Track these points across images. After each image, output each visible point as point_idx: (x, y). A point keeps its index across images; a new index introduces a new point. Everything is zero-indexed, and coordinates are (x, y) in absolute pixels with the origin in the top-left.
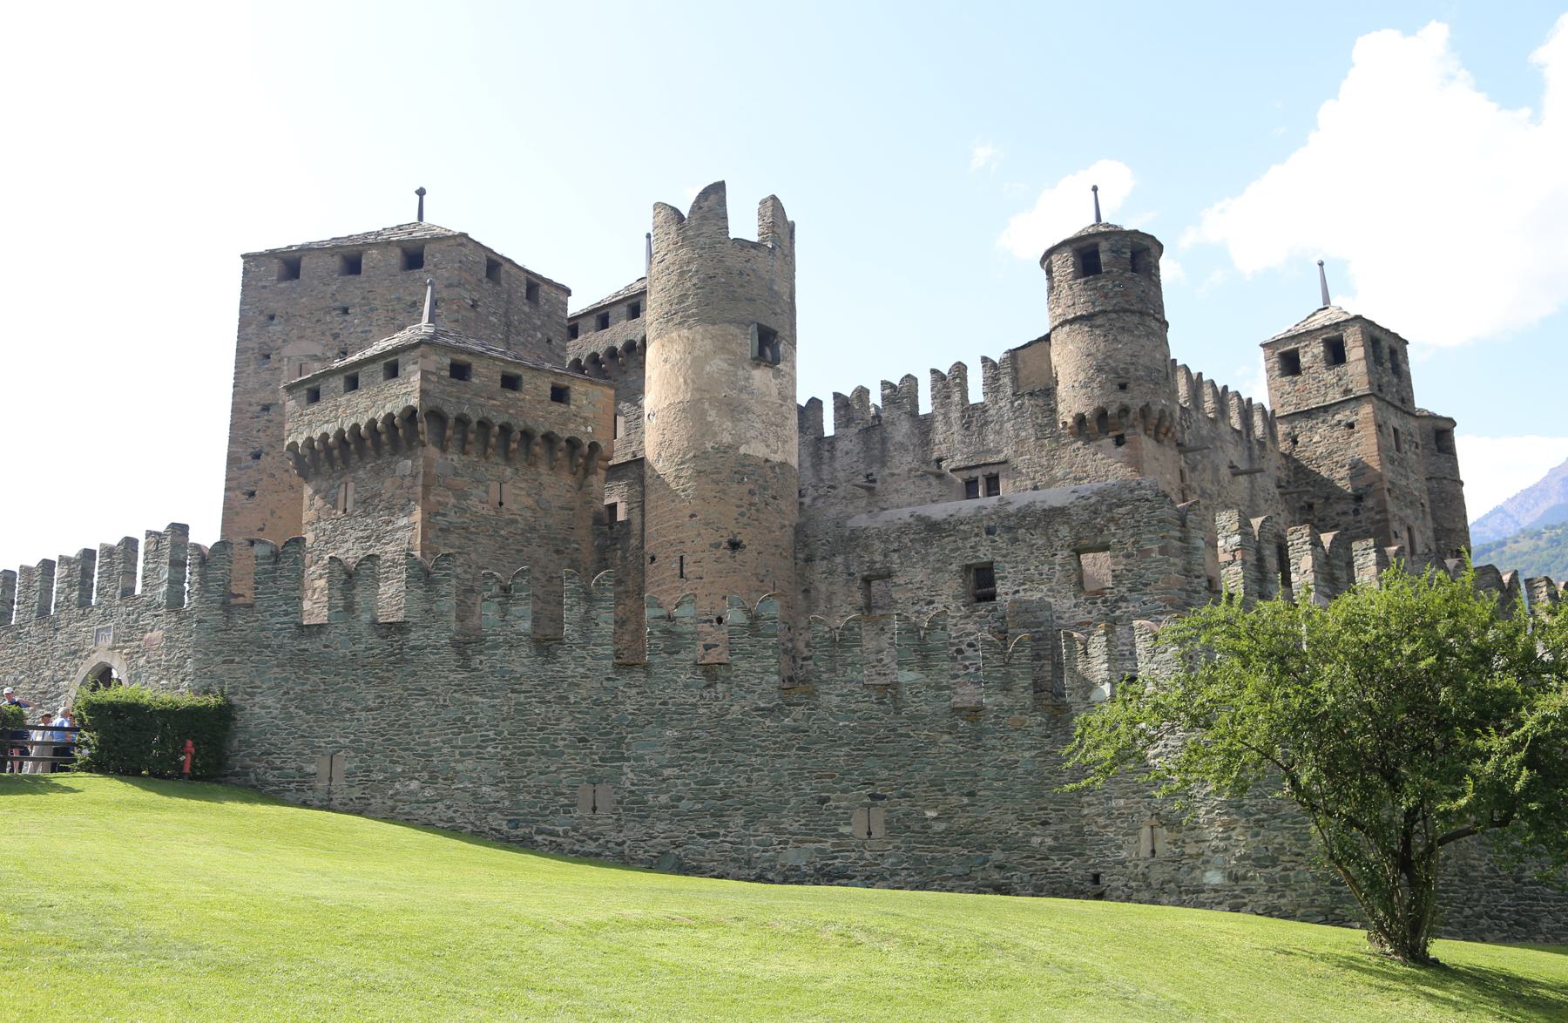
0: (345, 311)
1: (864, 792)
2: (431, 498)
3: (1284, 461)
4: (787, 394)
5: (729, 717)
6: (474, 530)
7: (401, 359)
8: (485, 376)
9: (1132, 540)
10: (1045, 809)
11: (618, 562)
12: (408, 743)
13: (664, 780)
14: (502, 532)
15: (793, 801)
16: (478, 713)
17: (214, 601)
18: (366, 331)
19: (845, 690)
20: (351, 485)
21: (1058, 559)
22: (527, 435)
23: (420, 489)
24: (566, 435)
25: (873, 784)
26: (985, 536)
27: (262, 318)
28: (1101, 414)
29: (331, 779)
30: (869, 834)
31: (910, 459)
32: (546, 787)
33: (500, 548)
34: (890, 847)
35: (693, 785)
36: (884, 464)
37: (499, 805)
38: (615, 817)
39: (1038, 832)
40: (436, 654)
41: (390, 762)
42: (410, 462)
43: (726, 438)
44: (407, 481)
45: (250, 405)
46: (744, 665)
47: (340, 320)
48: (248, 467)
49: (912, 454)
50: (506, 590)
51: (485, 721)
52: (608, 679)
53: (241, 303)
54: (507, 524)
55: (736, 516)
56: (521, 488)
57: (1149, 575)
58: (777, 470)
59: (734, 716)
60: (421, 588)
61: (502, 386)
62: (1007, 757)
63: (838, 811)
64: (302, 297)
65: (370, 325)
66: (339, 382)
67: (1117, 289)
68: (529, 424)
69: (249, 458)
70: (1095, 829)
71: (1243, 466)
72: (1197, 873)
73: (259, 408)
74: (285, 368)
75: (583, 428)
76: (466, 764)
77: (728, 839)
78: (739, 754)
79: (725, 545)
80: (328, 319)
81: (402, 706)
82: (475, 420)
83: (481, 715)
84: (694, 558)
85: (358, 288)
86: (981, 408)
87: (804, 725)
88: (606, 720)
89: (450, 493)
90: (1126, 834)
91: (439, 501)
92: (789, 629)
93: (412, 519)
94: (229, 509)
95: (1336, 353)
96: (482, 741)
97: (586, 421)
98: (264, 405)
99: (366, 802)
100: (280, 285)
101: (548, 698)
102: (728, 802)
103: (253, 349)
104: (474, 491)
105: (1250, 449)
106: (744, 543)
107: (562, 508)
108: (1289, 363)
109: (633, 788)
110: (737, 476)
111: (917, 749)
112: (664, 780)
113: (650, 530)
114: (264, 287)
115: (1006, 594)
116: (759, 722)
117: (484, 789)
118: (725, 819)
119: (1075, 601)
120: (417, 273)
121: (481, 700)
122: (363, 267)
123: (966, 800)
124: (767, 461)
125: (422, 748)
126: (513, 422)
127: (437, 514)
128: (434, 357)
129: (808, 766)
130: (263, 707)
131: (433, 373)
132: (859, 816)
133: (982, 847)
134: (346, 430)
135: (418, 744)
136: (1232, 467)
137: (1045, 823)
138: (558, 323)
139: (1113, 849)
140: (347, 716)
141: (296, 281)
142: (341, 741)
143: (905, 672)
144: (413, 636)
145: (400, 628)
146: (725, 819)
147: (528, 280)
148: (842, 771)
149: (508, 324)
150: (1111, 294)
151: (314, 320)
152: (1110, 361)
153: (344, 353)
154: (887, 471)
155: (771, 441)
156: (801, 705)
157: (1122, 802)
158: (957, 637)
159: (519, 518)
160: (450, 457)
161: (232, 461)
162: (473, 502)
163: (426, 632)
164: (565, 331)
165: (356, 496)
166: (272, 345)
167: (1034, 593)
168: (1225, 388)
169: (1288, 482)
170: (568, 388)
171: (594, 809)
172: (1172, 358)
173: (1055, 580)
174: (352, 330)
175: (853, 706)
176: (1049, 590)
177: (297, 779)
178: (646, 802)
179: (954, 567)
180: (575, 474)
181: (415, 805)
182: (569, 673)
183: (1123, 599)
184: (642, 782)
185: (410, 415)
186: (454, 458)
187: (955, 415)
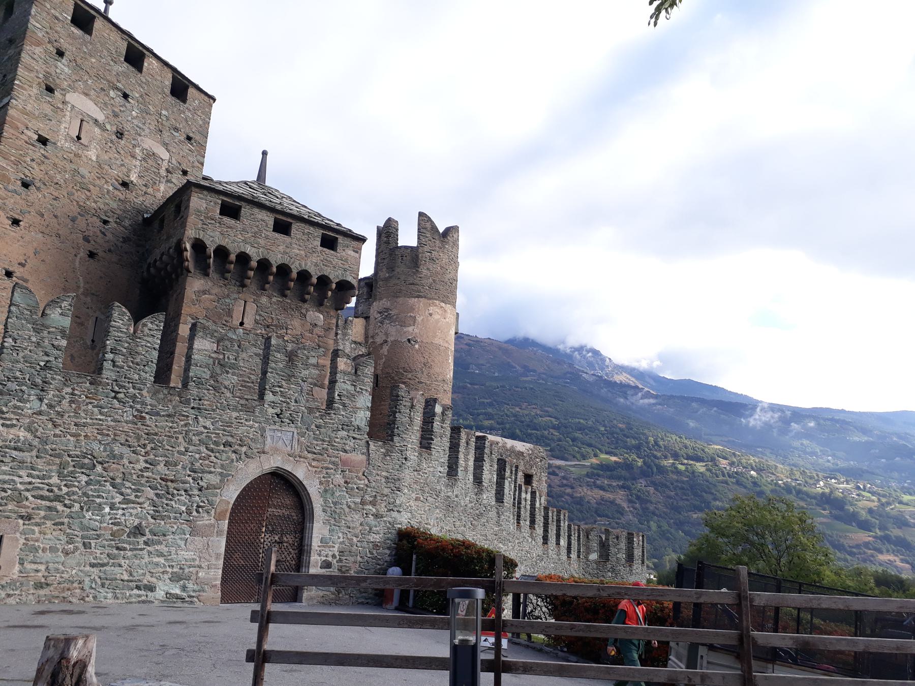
7: (341, 239)
20: (251, 308)
42: (322, 316)
44: (317, 330)
47: (122, 100)
48: (15, 192)
64: (91, 56)
65: (144, 124)
66: (269, 219)
69: (19, 183)
74: (68, 113)
80: (112, 93)
85: (140, 85)
98: (39, 135)
114: (57, 18)
120: (182, 106)
122: (144, 69)
134: (273, 262)
141: (87, 37)
153: (122, 134)
165: (258, 318)
166: (58, 81)
174: (130, 118)
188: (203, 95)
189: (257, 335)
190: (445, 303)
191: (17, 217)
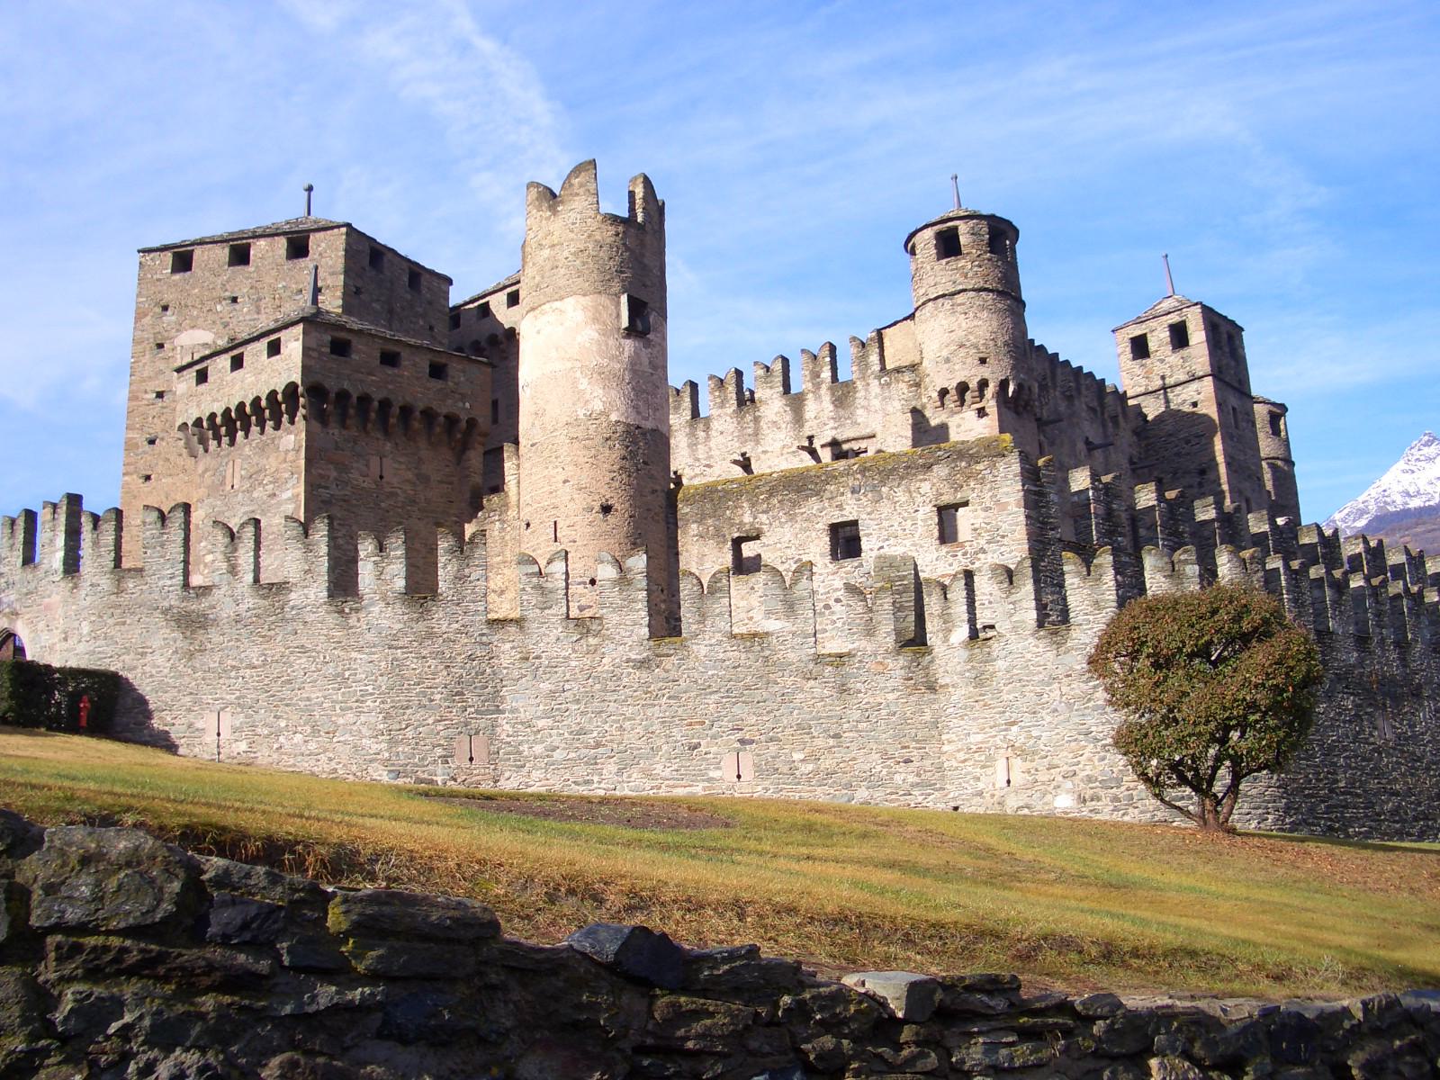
0: (234, 300)
1: (733, 737)
2: (313, 471)
3: (1135, 438)
4: (659, 365)
5: (599, 669)
6: (354, 502)
8: (363, 353)
9: (990, 494)
10: (907, 747)
11: (496, 533)
12: (291, 699)
13: (539, 731)
14: (383, 505)
15: (665, 747)
16: (356, 669)
17: (106, 566)
18: (254, 320)
19: (713, 641)
21: (920, 515)
22: (406, 411)
23: (303, 462)
24: (444, 411)
25: (742, 730)
26: (849, 495)
27: (159, 310)
28: (963, 388)
29: (219, 734)
30: (739, 777)
31: (783, 437)
32: (424, 739)
33: (381, 520)
34: (760, 788)
35: (566, 735)
36: (758, 442)
37: (379, 757)
38: (493, 767)
39: (900, 770)
40: (314, 613)
41: (275, 717)
43: (598, 406)
44: (291, 456)
45: (146, 392)
46: (615, 618)
48: (145, 453)
49: (784, 431)
50: (381, 548)
51: (364, 676)
52: (483, 635)
53: (137, 296)
54: (388, 497)
55: (607, 480)
56: (400, 463)
57: (1004, 526)
58: (648, 436)
59: (606, 668)
60: (300, 549)
61: (381, 363)
62: (871, 700)
63: (708, 756)
64: (194, 288)
66: (224, 361)
67: (975, 269)
68: (408, 399)
69: (146, 443)
70: (955, 764)
71: (1097, 440)
72: (1049, 797)
73: (154, 395)
74: (178, 356)
75: (461, 404)
76: (347, 717)
77: (602, 785)
78: (612, 704)
79: (597, 508)
80: (219, 308)
81: (284, 663)
82: (355, 397)
83: (360, 670)
84: (568, 523)
85: (247, 278)
86: (849, 386)
87: (673, 675)
88: (483, 673)
89: (331, 467)
90: (983, 767)
91: (320, 474)
92: (662, 591)
93: (296, 491)
94: (127, 493)
95: (1179, 336)
96: (362, 696)
97: (463, 397)
99: (252, 755)
100: (177, 277)
101: (424, 652)
102: (601, 750)
103: (148, 339)
104: (355, 465)
105: (1104, 426)
106: (617, 506)
107: (441, 482)
108: (1140, 348)
109: (509, 739)
110: (609, 442)
111: (783, 695)
112: (539, 731)
113: (525, 498)
114: (159, 280)
115: (871, 550)
116: (629, 674)
117: (364, 740)
118: (599, 766)
119: (936, 554)
120: (302, 262)
121: (359, 656)
122: (252, 258)
123: (831, 742)
124: (638, 427)
125: (304, 703)
126: (392, 397)
127: (320, 486)
128: (314, 334)
129: (679, 713)
130: (155, 666)
131: (314, 350)
132: (729, 762)
133: (849, 786)
135: (300, 700)
136: (1088, 442)
137: (908, 761)
138: (440, 311)
139: (971, 782)
140: (233, 674)
141: (189, 273)
142: (228, 697)
143: (772, 621)
144: (293, 596)
145: (280, 588)
146: (599, 766)
147: (410, 269)
148: (711, 718)
149: (391, 311)
150: (970, 275)
151: (205, 310)
152: (971, 338)
154: (760, 449)
155: (642, 409)
156: (671, 655)
157: (980, 738)
158: (825, 593)
159: (399, 491)
160: (331, 432)
161: (130, 446)
162: (354, 475)
163: (306, 591)
164: (447, 318)
165: (243, 472)
166: (166, 334)
167: (898, 548)
168: (1080, 368)
169: (1140, 459)
170: (445, 365)
171: (471, 759)
172: (1029, 337)
173: (917, 535)
174: (241, 318)
175: (721, 655)
176: (912, 545)
177: (187, 734)
178: (520, 753)
179: (820, 526)
180: (453, 449)
181: (300, 758)
182: (444, 628)
183: (983, 551)
184: (516, 734)
185: (291, 389)
186: (335, 431)
187: (824, 390)
188: (329, 232)
189: (243, 492)
190: (562, 299)
191: (149, 473)
